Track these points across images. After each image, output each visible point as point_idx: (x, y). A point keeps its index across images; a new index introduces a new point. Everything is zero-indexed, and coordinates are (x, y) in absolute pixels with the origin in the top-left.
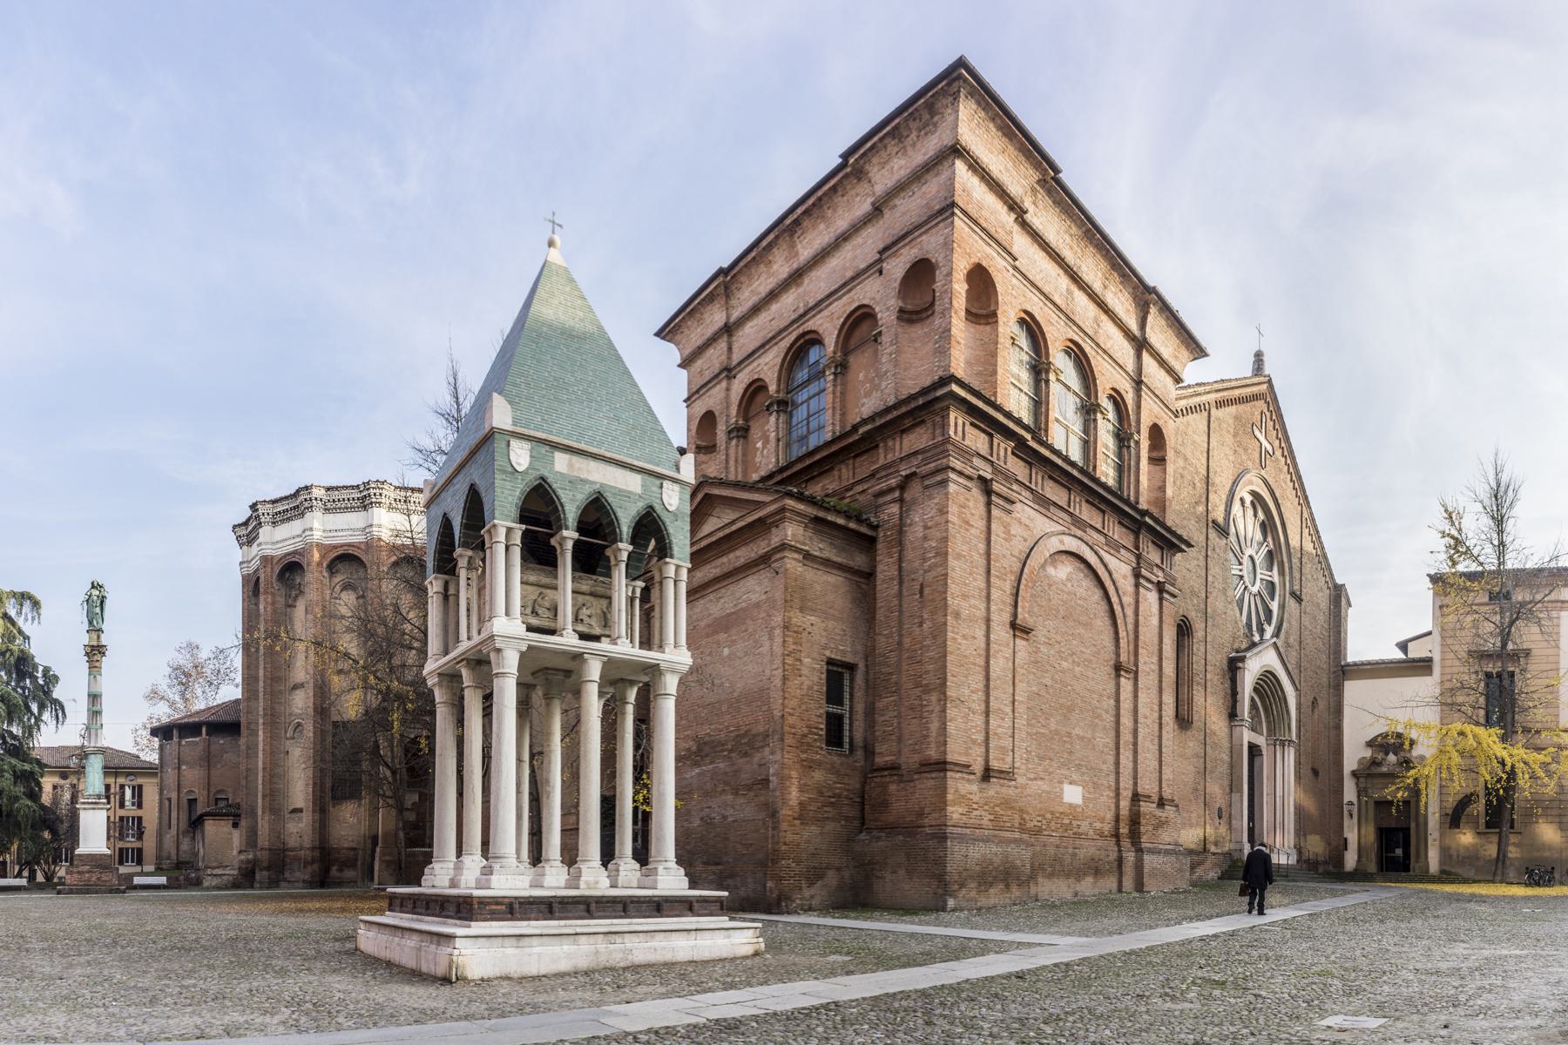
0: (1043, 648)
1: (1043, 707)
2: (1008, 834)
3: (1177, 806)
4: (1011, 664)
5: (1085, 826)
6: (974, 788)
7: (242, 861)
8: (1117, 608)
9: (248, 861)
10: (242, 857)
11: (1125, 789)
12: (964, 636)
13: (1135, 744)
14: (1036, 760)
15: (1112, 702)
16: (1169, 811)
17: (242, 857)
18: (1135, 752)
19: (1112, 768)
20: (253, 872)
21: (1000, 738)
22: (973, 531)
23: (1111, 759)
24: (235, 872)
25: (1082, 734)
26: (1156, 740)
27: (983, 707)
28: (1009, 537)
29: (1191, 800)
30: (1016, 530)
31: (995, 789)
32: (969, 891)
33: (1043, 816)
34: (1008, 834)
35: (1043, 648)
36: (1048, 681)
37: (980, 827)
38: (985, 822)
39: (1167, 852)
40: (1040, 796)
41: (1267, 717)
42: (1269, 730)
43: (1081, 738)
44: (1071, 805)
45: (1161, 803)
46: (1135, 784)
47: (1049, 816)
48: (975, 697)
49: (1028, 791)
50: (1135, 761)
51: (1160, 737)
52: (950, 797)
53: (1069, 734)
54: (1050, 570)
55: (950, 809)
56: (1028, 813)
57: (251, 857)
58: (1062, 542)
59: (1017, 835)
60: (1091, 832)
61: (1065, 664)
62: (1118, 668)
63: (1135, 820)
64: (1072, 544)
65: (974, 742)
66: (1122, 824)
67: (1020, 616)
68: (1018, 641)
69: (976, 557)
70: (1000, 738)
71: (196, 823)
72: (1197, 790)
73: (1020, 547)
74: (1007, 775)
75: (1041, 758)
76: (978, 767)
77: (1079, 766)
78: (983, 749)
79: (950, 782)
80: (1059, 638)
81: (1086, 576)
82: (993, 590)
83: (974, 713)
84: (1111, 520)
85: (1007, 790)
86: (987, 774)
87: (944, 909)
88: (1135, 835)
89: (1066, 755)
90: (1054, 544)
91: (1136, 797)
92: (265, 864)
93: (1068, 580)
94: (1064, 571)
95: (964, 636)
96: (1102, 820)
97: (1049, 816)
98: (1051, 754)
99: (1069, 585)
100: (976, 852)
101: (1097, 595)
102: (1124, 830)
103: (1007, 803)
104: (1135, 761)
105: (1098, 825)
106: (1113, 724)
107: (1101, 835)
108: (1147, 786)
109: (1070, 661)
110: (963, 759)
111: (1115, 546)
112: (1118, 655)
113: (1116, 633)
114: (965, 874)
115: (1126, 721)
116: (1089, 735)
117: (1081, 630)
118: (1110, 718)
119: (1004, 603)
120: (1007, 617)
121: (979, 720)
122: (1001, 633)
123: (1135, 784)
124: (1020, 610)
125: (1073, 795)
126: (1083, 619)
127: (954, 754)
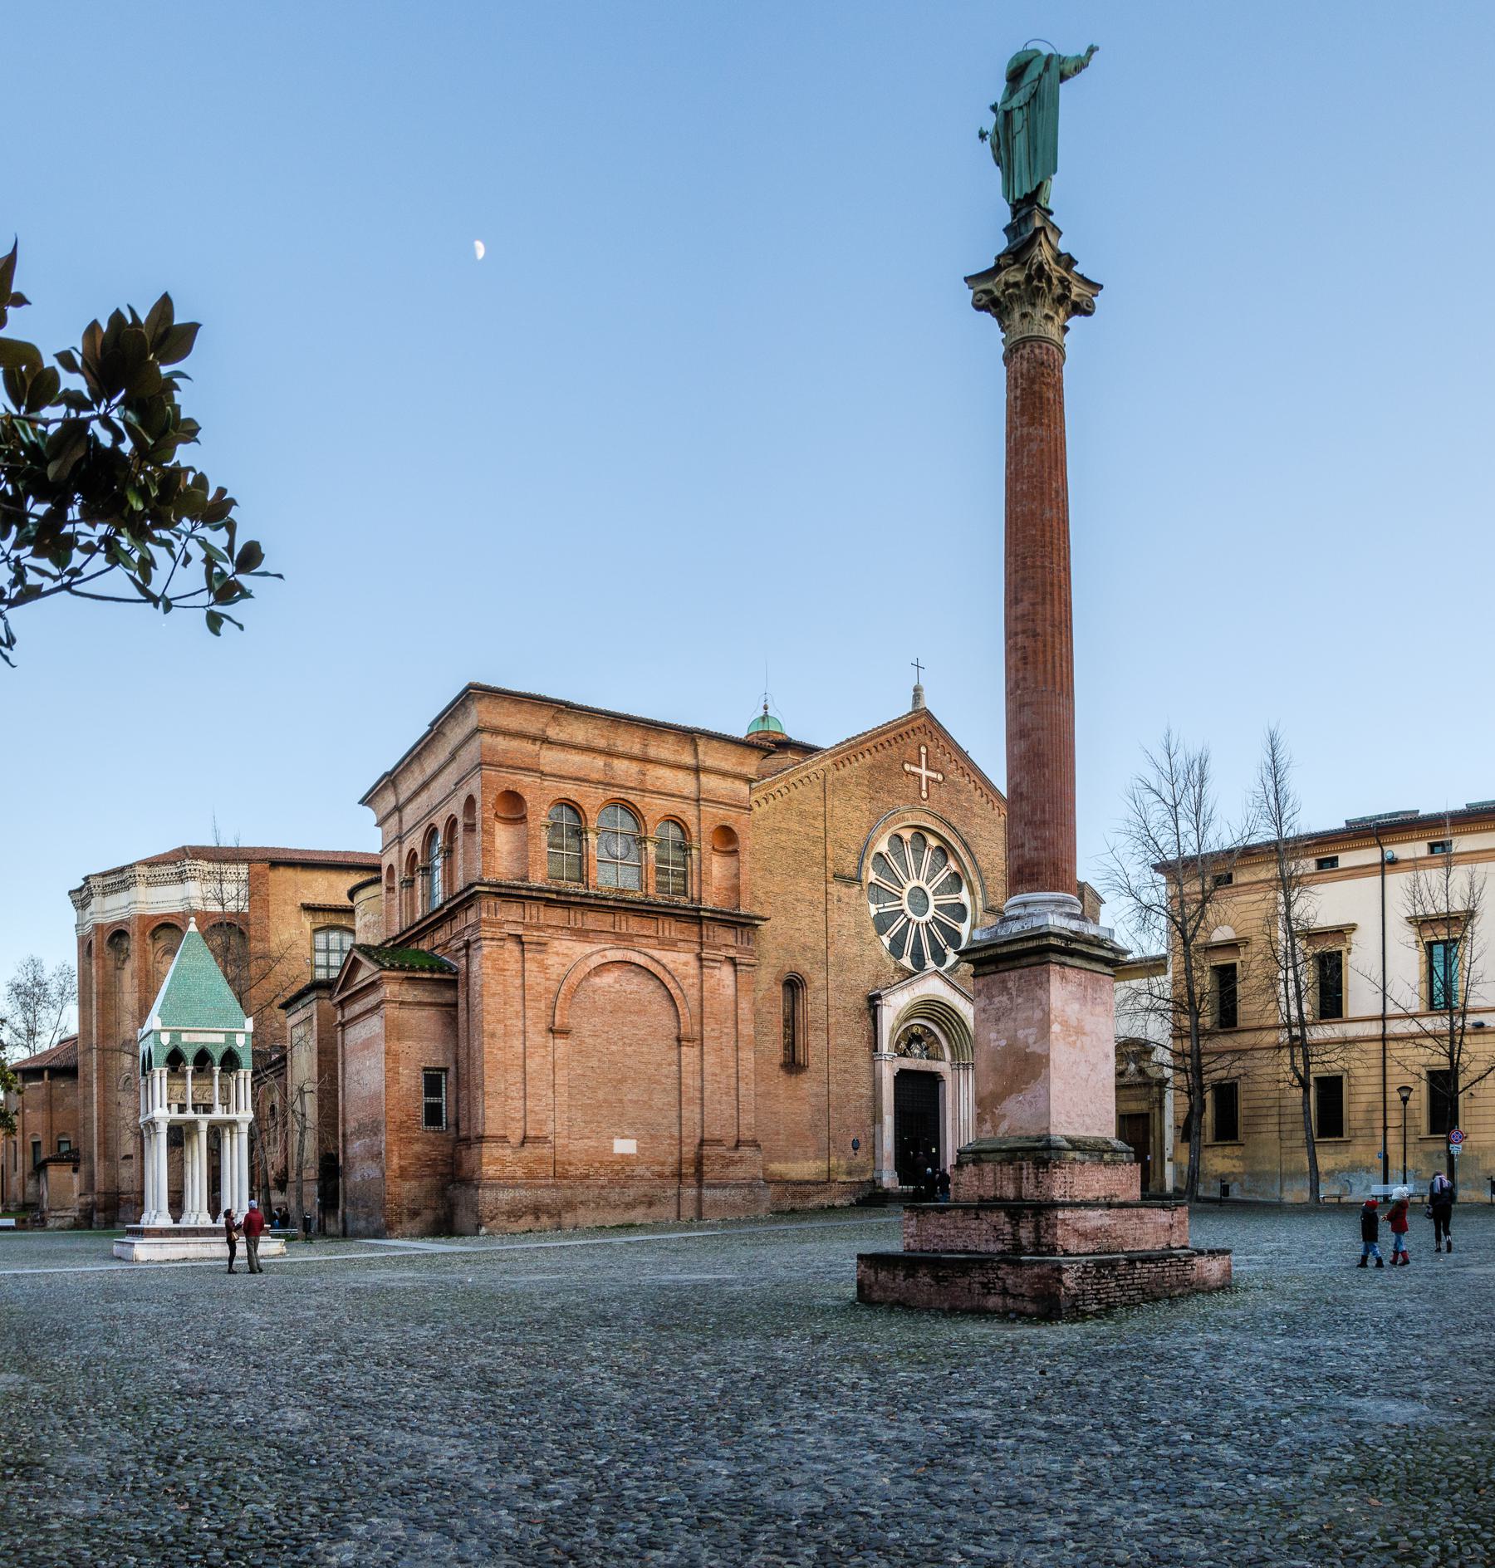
0: (589, 1040)
1: (589, 1084)
2: (543, 1182)
3: (759, 1146)
4: (550, 1058)
5: (640, 1170)
6: (508, 1151)
7: (82, 1204)
8: (675, 992)
9: (88, 1204)
10: (83, 1200)
11: (689, 1137)
12: (499, 1049)
13: (702, 1099)
14: (582, 1125)
15: (675, 1068)
16: (746, 1151)
17: (83, 1200)
18: (702, 1105)
19: (676, 1121)
20: (92, 1213)
21: (536, 1114)
22: (508, 973)
23: (674, 1114)
24: (76, 1214)
25: (635, 1098)
26: (733, 1092)
27: (522, 1094)
28: (544, 968)
29: (807, 1137)
30: (551, 960)
31: (528, 1151)
32: (501, 1221)
33: (592, 1166)
34: (543, 1182)
35: (589, 1040)
36: (594, 1063)
37: (513, 1178)
38: (519, 1174)
39: (738, 1186)
40: (586, 1151)
41: (949, 1042)
42: (953, 1054)
43: (636, 1102)
44: (622, 1155)
45: (738, 1144)
46: (703, 1132)
47: (597, 1165)
48: (513, 1088)
49: (571, 1147)
50: (702, 1113)
51: (737, 1089)
52: (484, 1160)
53: (621, 1101)
54: (596, 981)
55: (485, 1168)
56: (570, 1164)
57: (89, 1199)
58: (605, 956)
59: (551, 1181)
60: (648, 1174)
61: (614, 1048)
62: (679, 1040)
63: (699, 1162)
64: (618, 955)
65: (513, 1119)
66: (684, 1166)
67: (557, 1023)
68: (557, 1041)
69: (512, 990)
70: (536, 1114)
71: (39, 1168)
72: (816, 1126)
73: (556, 971)
74: (540, 1140)
76: (515, 1139)
77: (632, 1124)
78: (522, 1123)
79: (484, 1150)
80: (606, 1029)
81: (637, 974)
82: (527, 1011)
83: (512, 1099)
84: (667, 926)
85: (546, 1150)
86: (525, 1140)
87: (478, 1234)
88: (699, 1174)
90: (597, 960)
91: (702, 1143)
92: (101, 1207)
94: (607, 979)
95: (499, 1049)
96: (663, 1164)
97: (597, 1165)
98: (599, 1118)
99: (617, 986)
100: (505, 1196)
101: (652, 985)
102: (689, 1170)
103: (540, 1160)
104: (702, 1113)
105: (657, 1168)
106: (677, 1086)
107: (661, 1176)
108: (714, 1131)
109: (621, 1043)
110: (501, 1132)
111: (670, 945)
112: (679, 1028)
113: (677, 1011)
114: (495, 1211)
115: (690, 1081)
116: (645, 1097)
117: (634, 1018)
118: (671, 1083)
119: (538, 1017)
120: (542, 1026)
121: (519, 1104)
122: (536, 1037)
123: (703, 1132)
124: (557, 1018)
125: (625, 1146)
126: (636, 1008)
127: (491, 1129)
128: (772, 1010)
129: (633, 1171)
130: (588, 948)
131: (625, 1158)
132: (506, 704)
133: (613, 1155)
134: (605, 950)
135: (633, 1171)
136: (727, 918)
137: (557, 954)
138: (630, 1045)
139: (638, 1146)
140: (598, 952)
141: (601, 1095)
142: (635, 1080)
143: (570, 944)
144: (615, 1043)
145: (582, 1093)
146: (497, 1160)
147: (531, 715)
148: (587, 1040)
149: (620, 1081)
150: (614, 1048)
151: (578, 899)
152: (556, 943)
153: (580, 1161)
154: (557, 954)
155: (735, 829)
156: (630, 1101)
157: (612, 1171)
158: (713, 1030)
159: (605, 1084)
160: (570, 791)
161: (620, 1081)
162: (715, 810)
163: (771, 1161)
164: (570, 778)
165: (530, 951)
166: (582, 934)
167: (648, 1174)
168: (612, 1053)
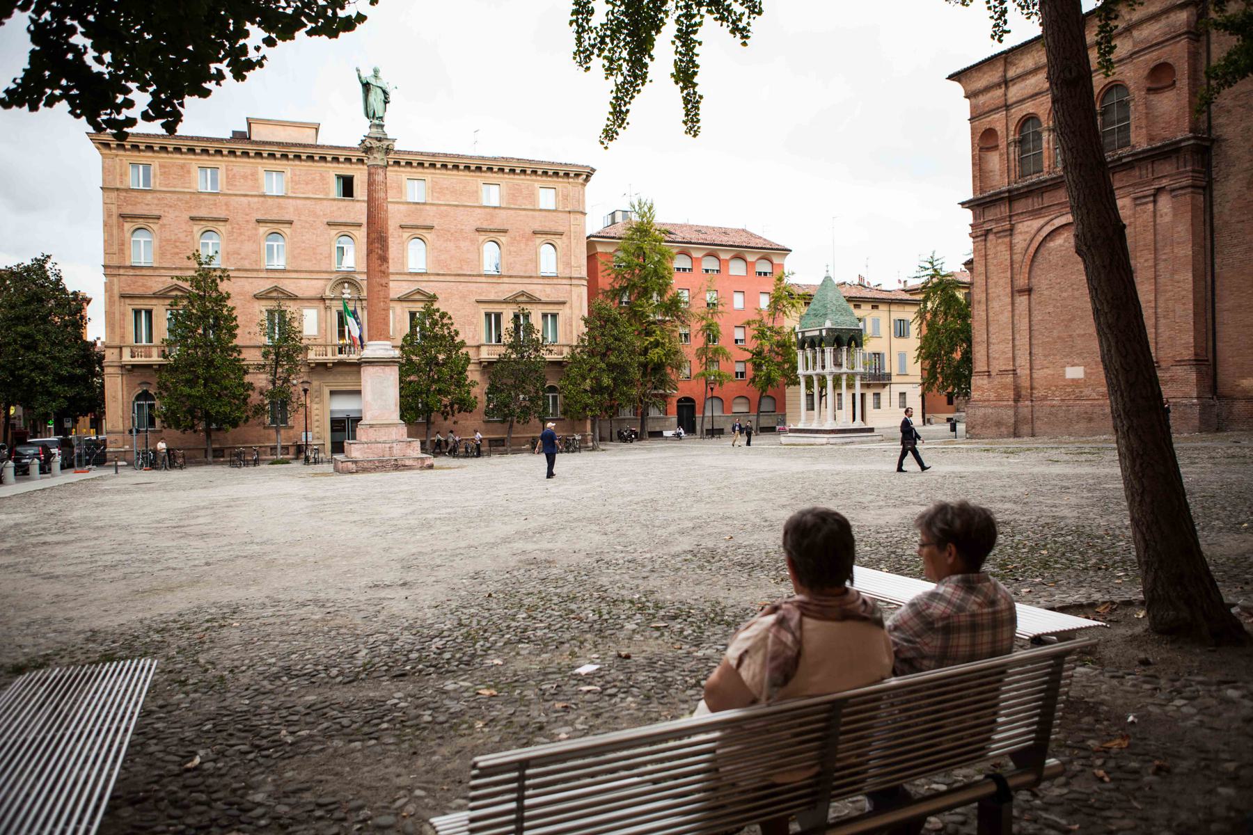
5: (1087, 392)
25: (1083, 332)
37: (988, 400)
38: (992, 398)
43: (1083, 335)
44: (1073, 380)
47: (1053, 388)
54: (1052, 244)
61: (1065, 295)
75: (1045, 356)
77: (1080, 354)
89: (1067, 350)
93: (1065, 241)
98: (1055, 352)
109: (1070, 289)
125: (1075, 372)
128: (1245, 218)
129: (1081, 392)
130: (1041, 221)
131: (1075, 382)
132: (974, 74)
133: (1065, 380)
134: (1052, 220)
135: (1081, 392)
136: (1149, 154)
137: (1021, 233)
138: (1078, 290)
139: (1085, 372)
140: (1047, 223)
141: (1055, 333)
142: (1082, 318)
143: (1029, 223)
144: (1066, 291)
145: (1041, 333)
146: (979, 388)
147: (992, 71)
148: (1045, 293)
149: (1070, 320)
150: (1065, 295)
151: (1025, 190)
152: (1020, 225)
153: (1042, 386)
154: (1021, 233)
155: (1170, 61)
156: (1079, 335)
157: (1065, 392)
158: (1146, 261)
159: (1058, 324)
160: (1029, 108)
161: (1070, 320)
162: (1147, 56)
163: (1244, 377)
164: (1028, 98)
165: (1000, 237)
166: (1035, 213)
167: (1094, 395)
168: (1064, 299)
